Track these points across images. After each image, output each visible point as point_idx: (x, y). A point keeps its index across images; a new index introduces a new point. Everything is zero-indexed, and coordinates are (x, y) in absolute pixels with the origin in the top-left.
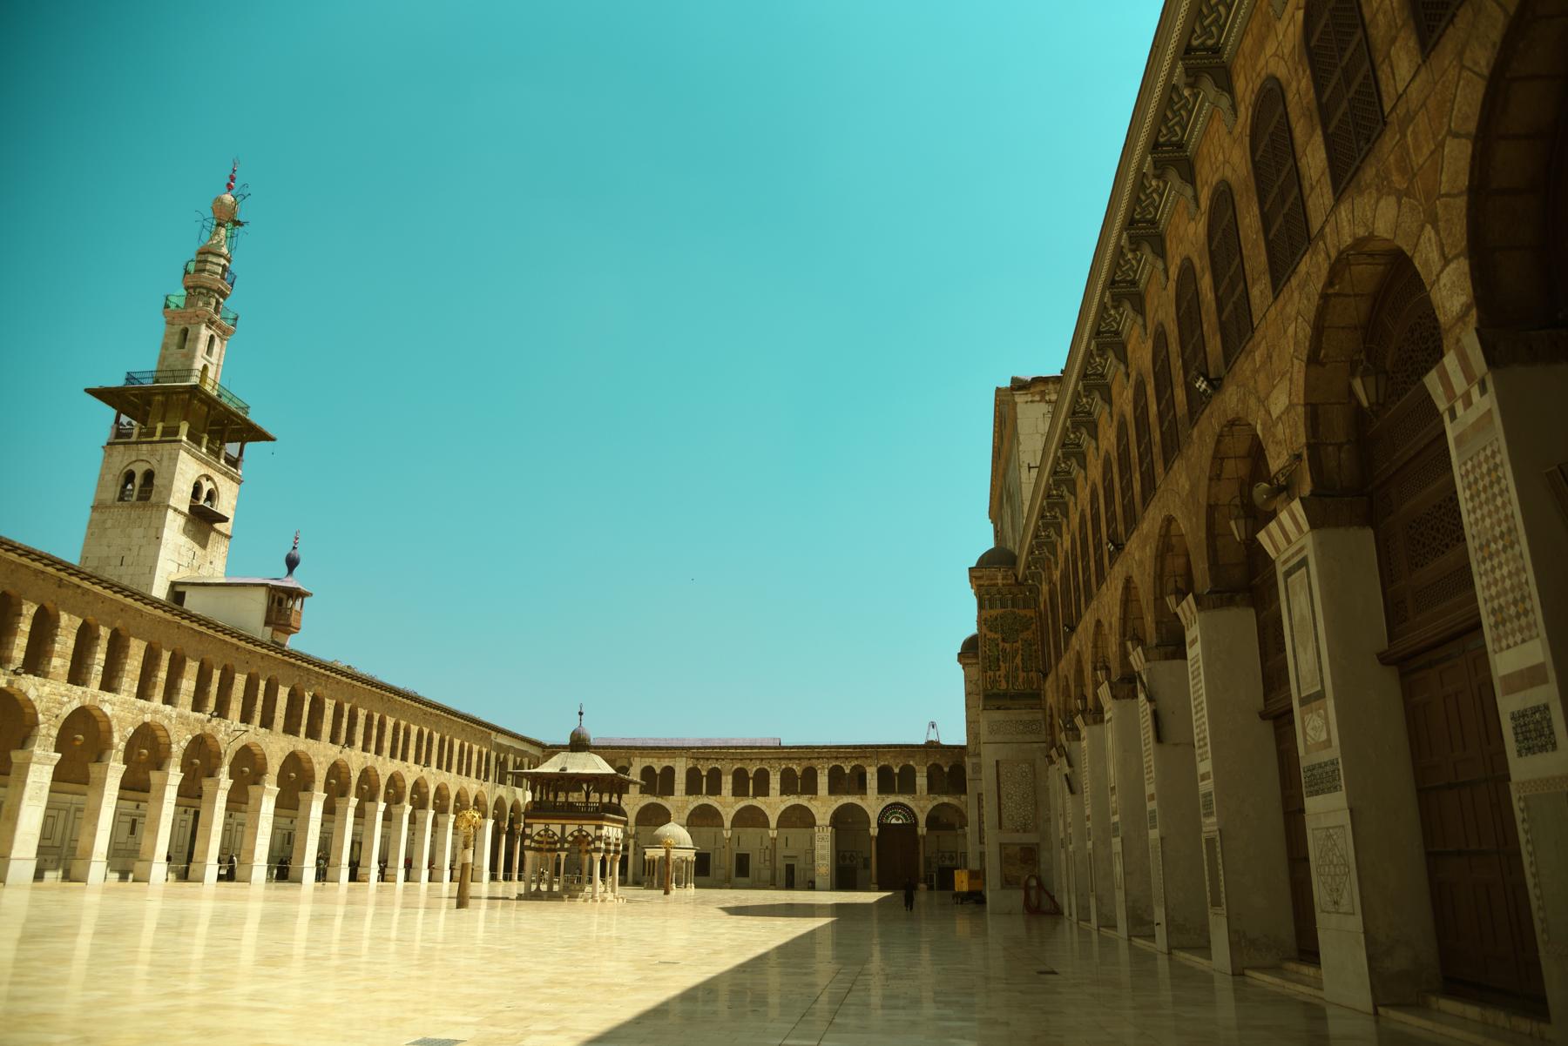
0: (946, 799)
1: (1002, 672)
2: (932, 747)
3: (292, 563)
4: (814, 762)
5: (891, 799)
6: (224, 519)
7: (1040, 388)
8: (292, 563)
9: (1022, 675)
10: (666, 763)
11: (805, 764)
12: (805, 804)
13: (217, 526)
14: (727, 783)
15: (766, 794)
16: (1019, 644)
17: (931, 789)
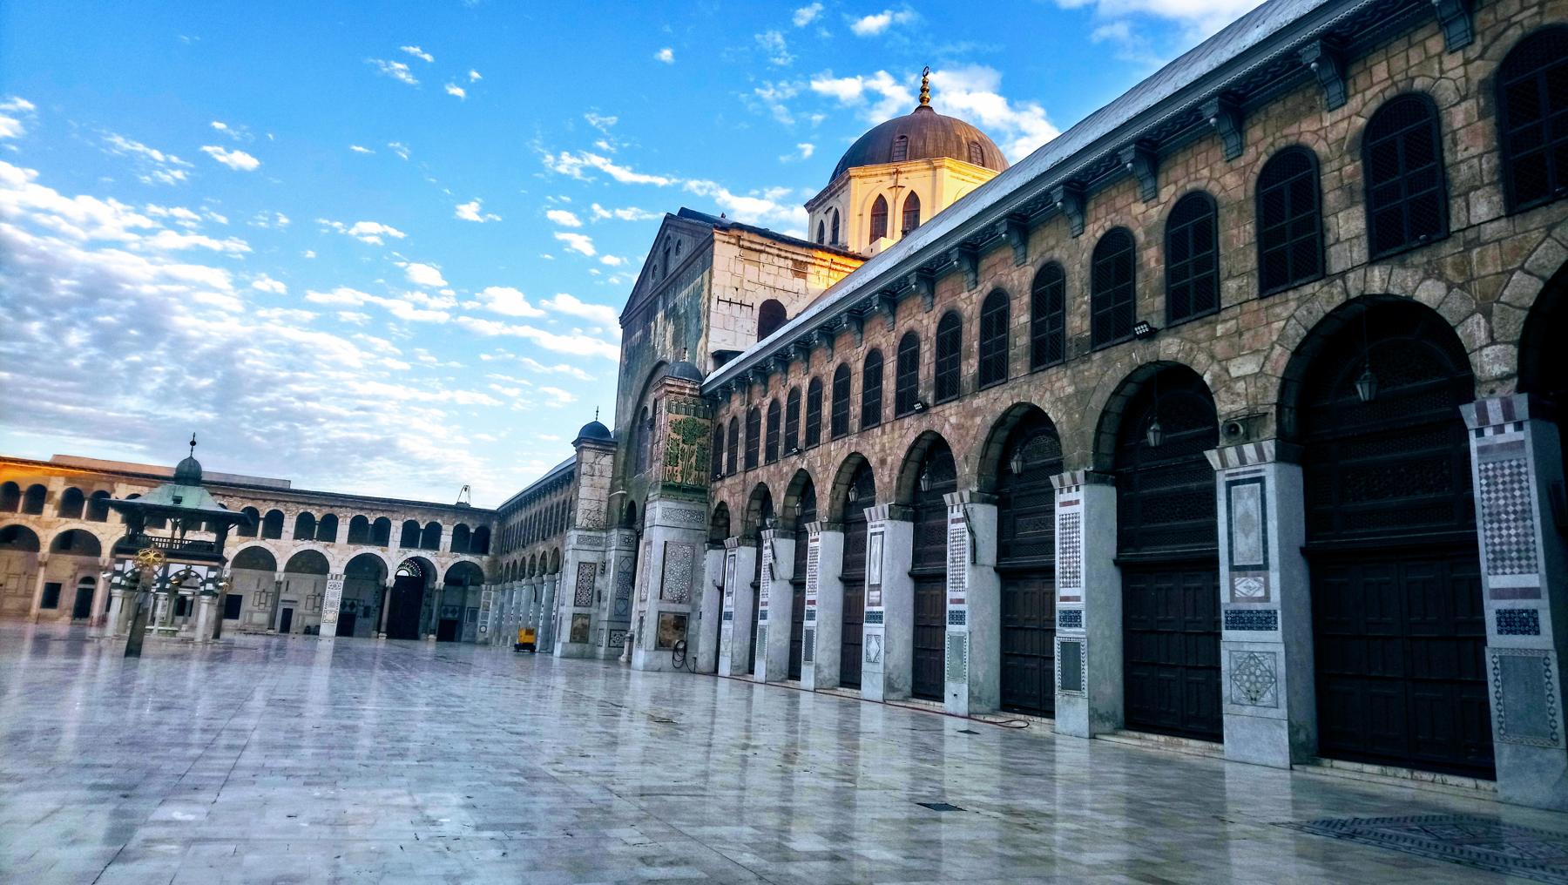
0: (467, 558)
1: (679, 468)
2: (461, 509)
4: (336, 511)
5: (413, 553)
7: (736, 233)
11: (326, 511)
12: (321, 550)
15: (278, 536)
17: (456, 547)
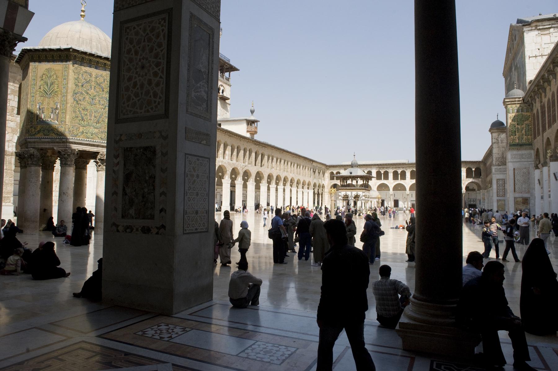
0: (473, 180)
1: (517, 136)
3: (252, 112)
6: (228, 99)
8: (252, 112)
9: (525, 137)
10: (369, 169)
13: (227, 101)
14: (391, 176)
16: (524, 126)
17: (467, 177)
